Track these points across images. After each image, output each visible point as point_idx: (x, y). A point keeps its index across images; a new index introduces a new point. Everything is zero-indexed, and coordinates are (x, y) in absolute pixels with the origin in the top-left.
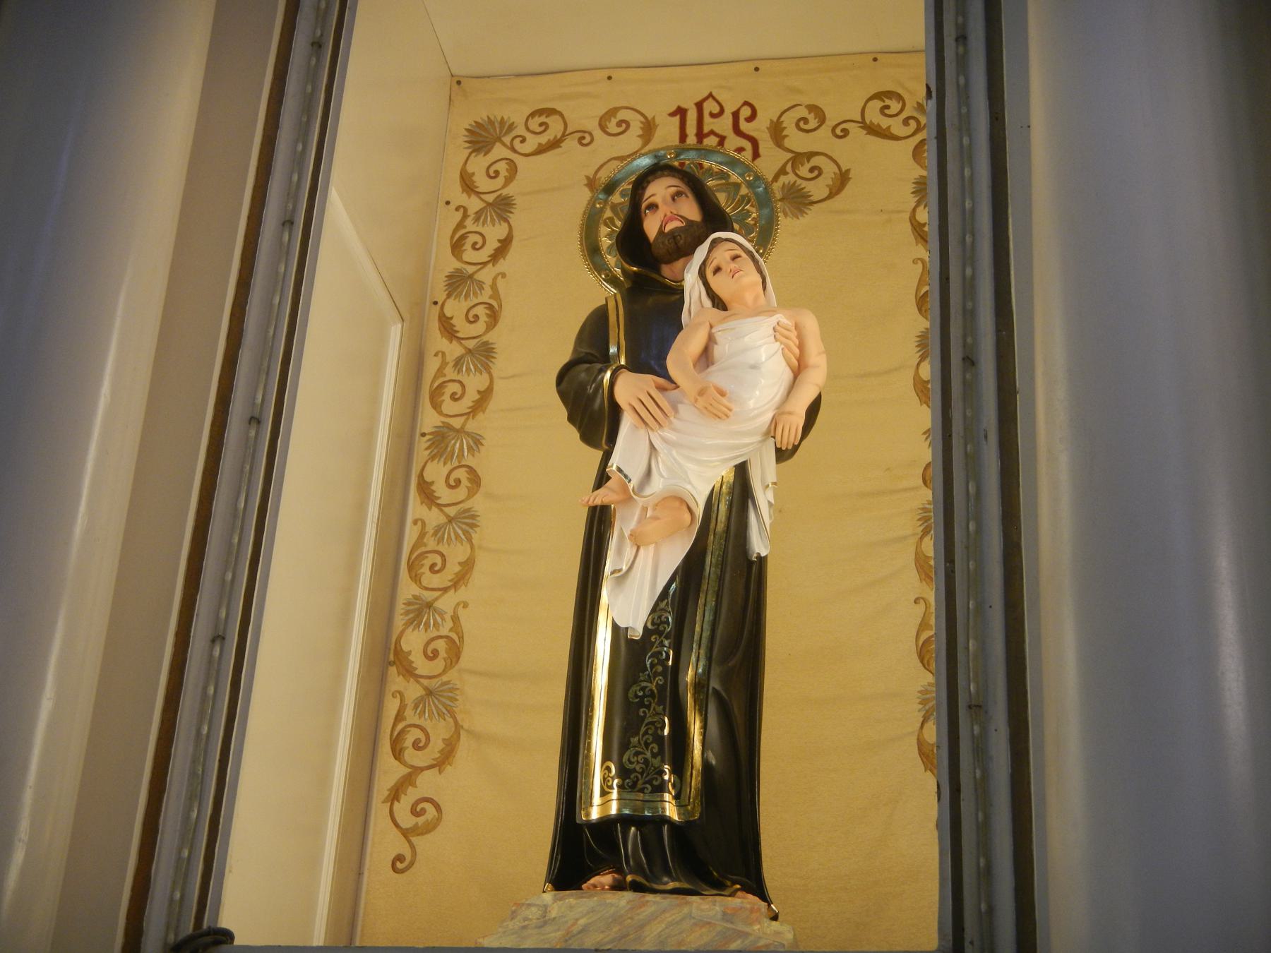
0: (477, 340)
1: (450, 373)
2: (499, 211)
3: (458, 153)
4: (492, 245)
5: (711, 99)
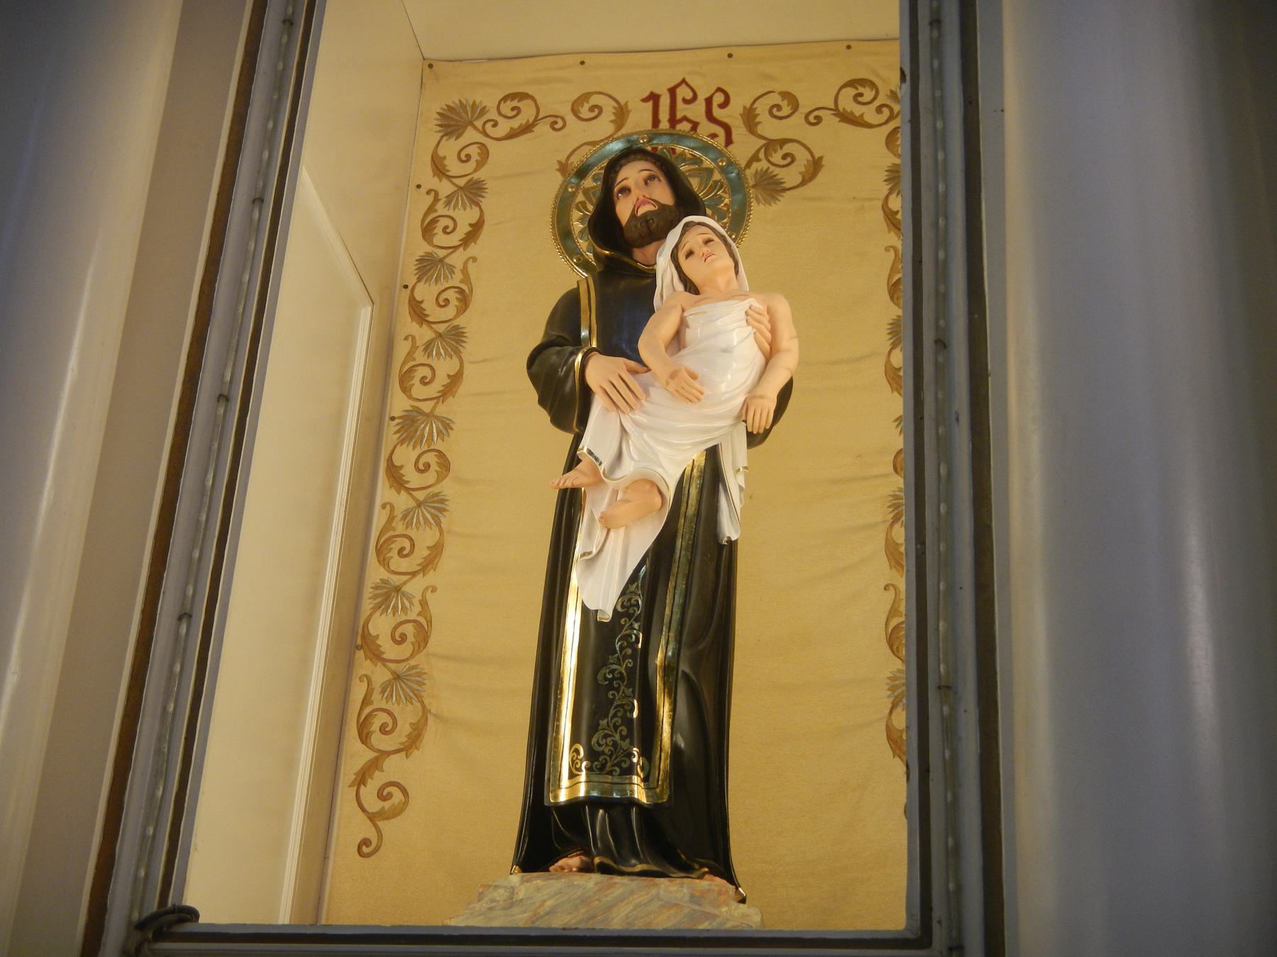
0: (447, 324)
1: (420, 357)
2: (471, 196)
3: (429, 136)
4: (463, 229)
5: (684, 85)
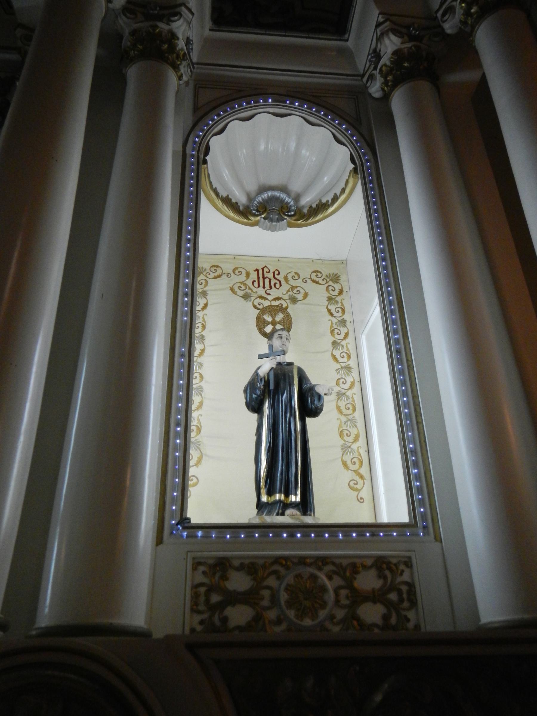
5: (266, 267)
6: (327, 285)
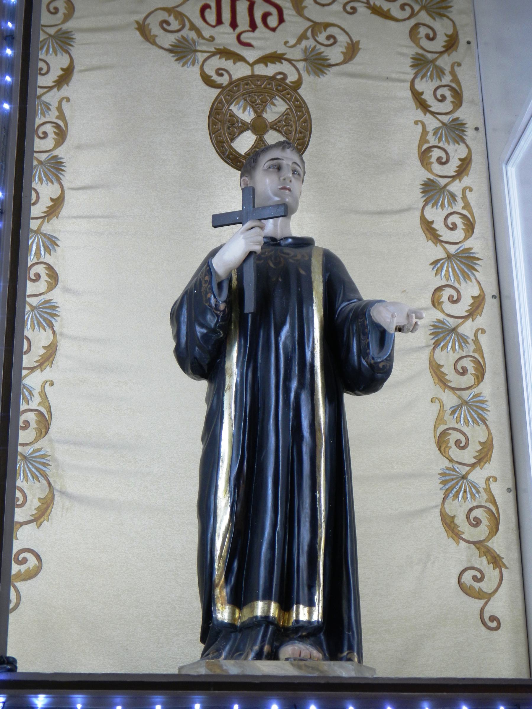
6: (412, 22)
